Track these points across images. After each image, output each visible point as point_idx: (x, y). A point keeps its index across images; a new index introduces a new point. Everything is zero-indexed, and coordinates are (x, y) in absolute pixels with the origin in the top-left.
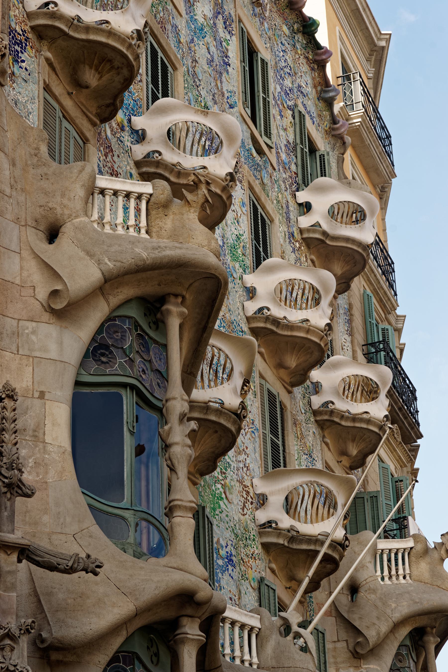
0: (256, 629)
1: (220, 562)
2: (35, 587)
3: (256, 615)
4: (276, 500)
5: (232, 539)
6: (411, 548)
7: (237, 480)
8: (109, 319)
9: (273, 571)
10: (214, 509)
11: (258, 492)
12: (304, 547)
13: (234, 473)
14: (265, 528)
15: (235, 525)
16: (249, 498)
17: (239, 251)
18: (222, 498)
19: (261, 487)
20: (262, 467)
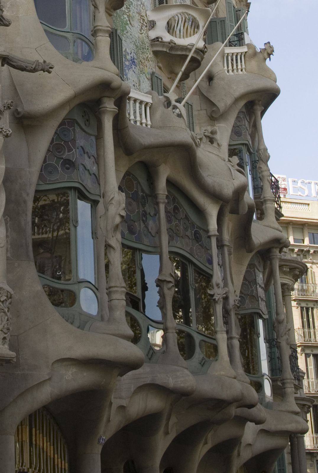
0: (149, 104)
1: (127, 63)
2: (13, 81)
3: (149, 96)
4: (161, 24)
5: (134, 49)
6: (246, 52)
7: (137, 13)
9: (160, 68)
10: (123, 31)
11: (150, 19)
12: (179, 53)
13: (135, 8)
14: (154, 42)
15: (136, 40)
16: (144, 23)
18: (127, 24)
19: (152, 16)
20: (152, 4)
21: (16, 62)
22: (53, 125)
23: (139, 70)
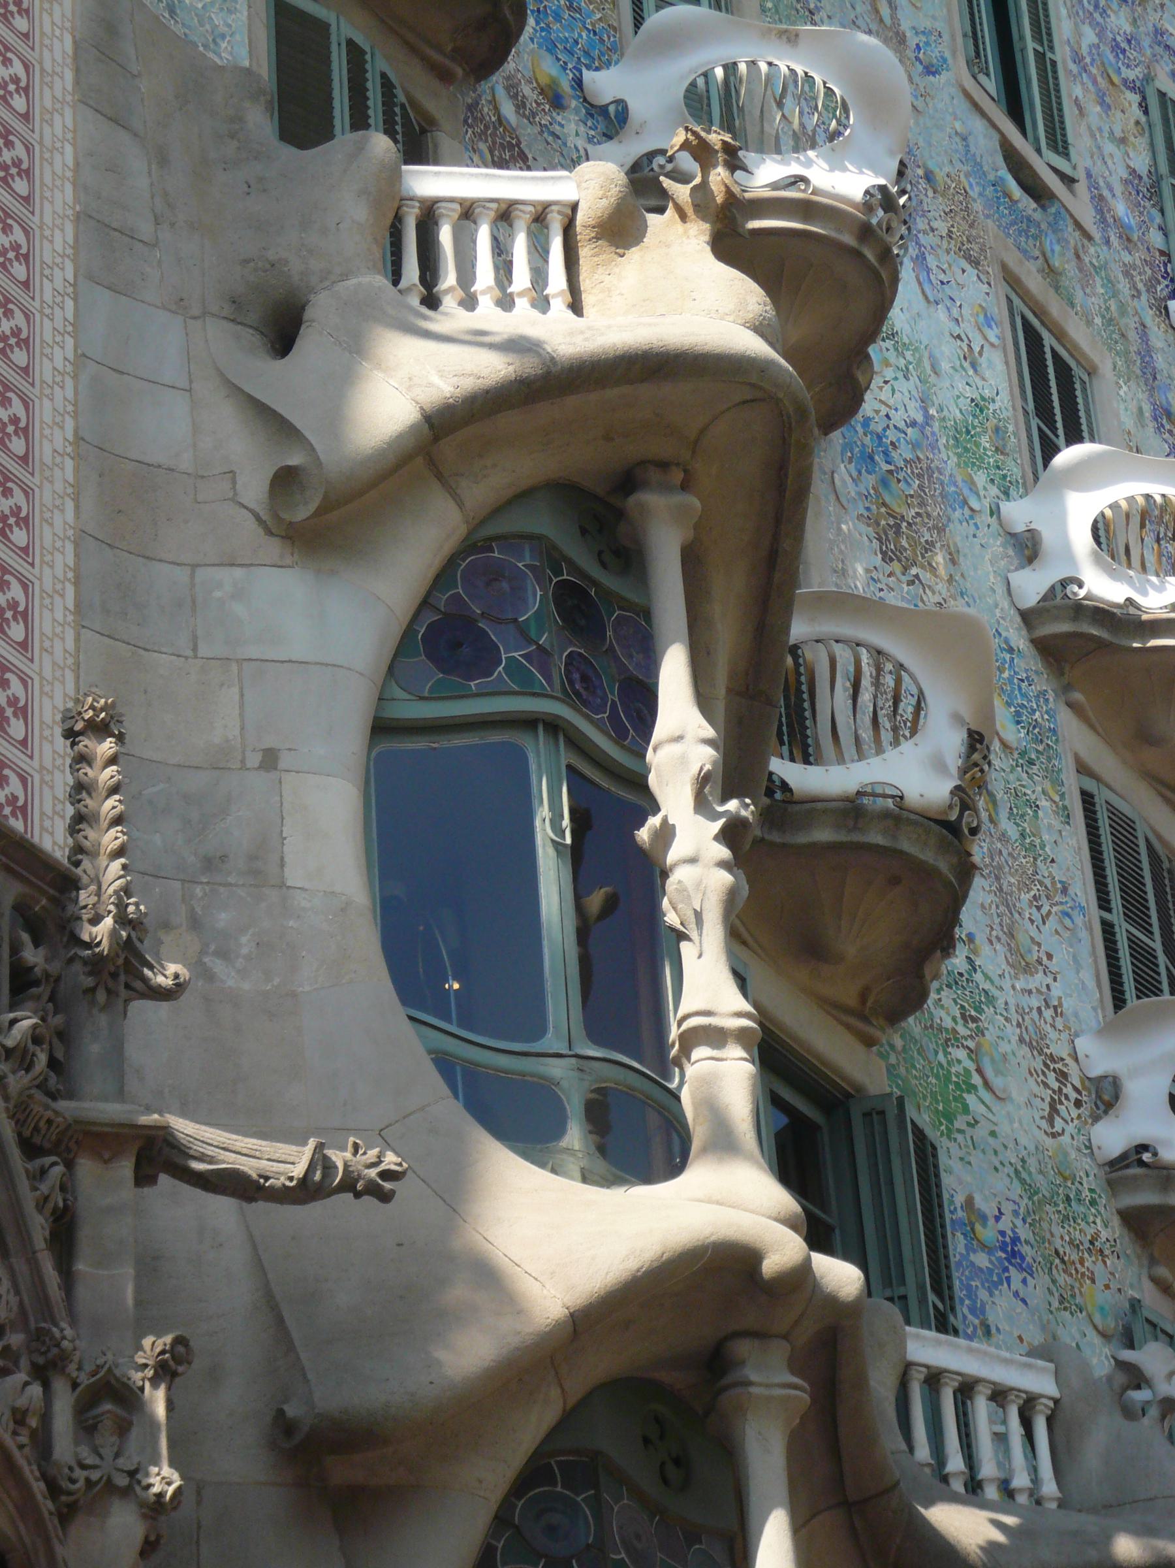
0: (1044, 1401)
1: (981, 1260)
2: (267, 1284)
3: (1040, 1363)
5: (1017, 1199)
7: (1021, 1040)
8: (472, 546)
10: (950, 1117)
11: (1094, 1073)
13: (1007, 1019)
14: (1127, 1166)
15: (1023, 1161)
16: (1068, 1090)
17: (985, 441)
18: (972, 1088)
19: (1098, 1056)
20: (1103, 1009)
21: (211, 1160)
22: (480, 1482)
23: (1051, 1292)
